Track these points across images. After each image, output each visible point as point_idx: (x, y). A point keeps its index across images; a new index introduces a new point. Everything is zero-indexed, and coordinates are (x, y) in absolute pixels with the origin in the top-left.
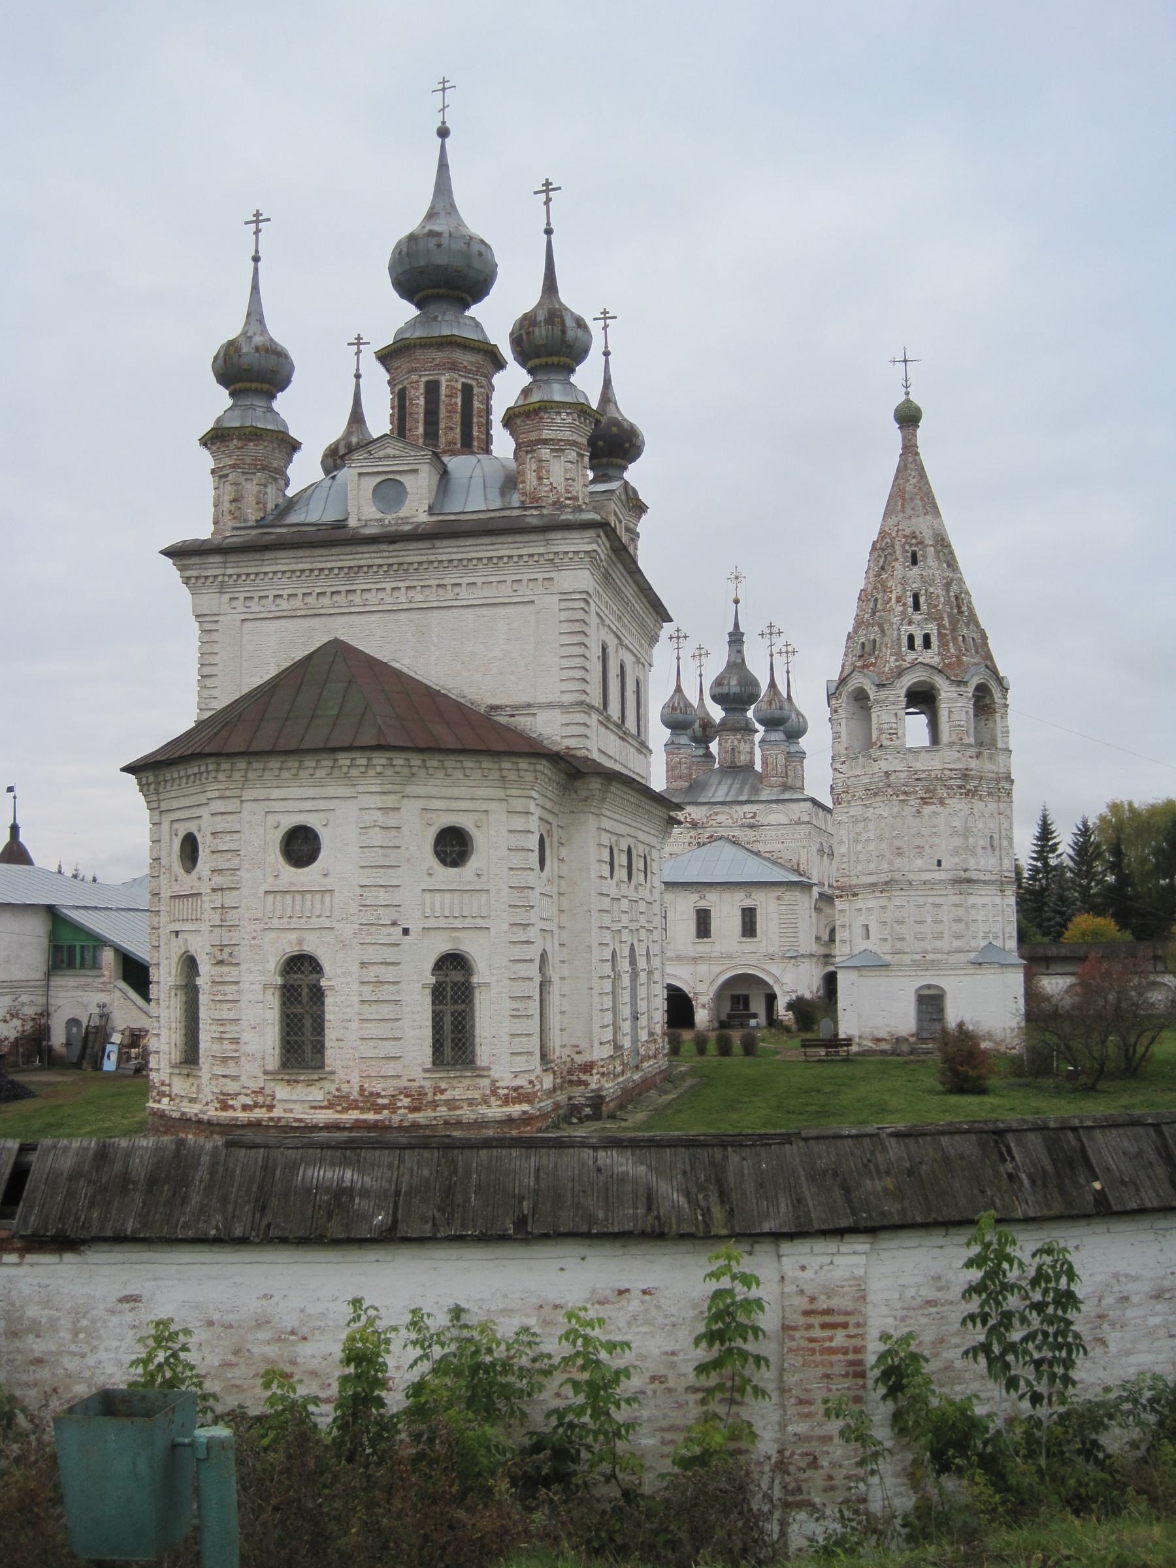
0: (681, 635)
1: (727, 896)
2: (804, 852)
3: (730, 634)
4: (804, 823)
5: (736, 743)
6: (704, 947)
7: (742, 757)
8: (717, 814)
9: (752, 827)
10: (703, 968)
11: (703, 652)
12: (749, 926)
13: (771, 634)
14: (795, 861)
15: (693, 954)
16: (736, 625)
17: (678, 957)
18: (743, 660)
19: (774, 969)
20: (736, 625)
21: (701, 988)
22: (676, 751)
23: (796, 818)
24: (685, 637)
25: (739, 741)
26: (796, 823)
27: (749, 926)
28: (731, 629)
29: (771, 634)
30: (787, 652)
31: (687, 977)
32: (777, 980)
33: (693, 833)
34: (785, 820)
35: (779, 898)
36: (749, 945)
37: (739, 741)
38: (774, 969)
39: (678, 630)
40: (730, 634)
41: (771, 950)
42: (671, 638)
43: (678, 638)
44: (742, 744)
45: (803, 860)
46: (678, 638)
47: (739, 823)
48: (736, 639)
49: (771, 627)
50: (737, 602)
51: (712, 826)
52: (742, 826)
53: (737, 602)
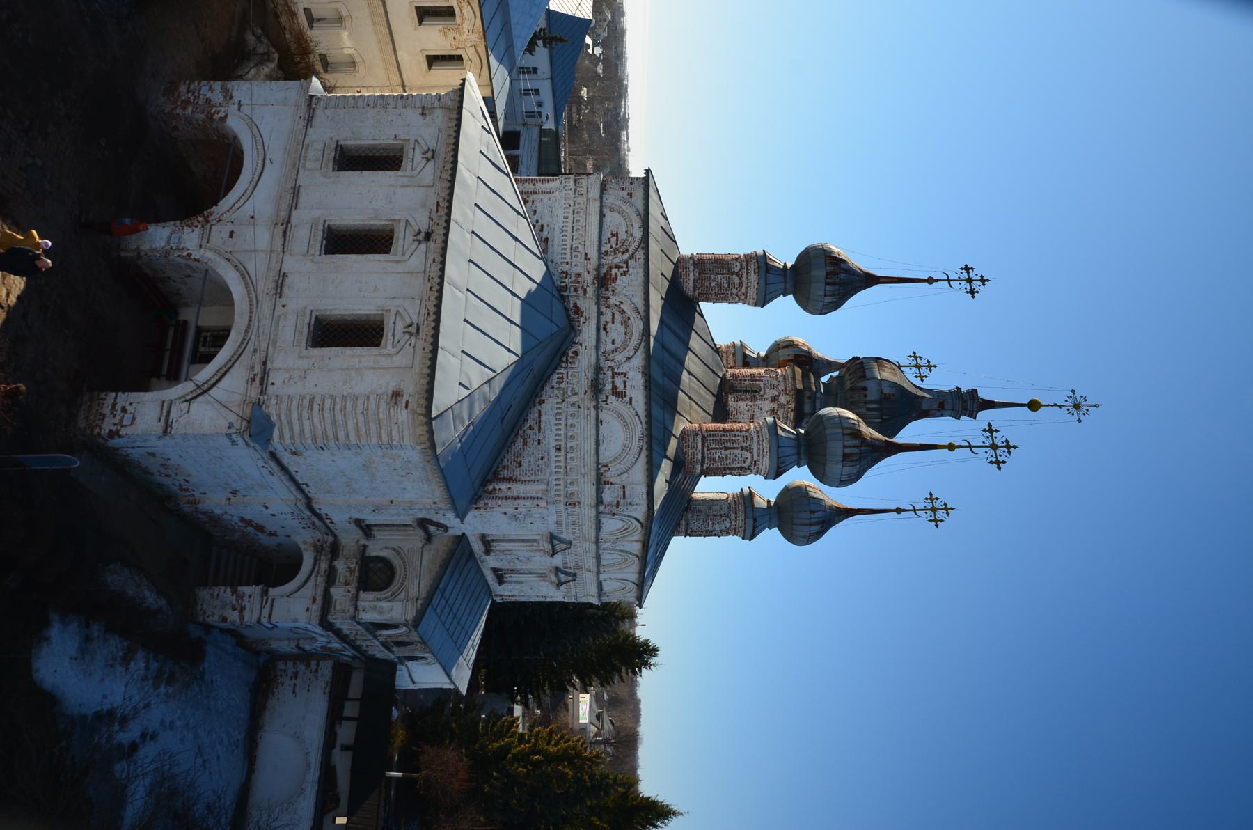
0: (975, 285)
1: (418, 285)
2: (534, 489)
3: (974, 392)
4: (599, 492)
5: (771, 393)
6: (305, 235)
7: (742, 405)
8: (625, 323)
9: (596, 388)
10: (263, 237)
11: (925, 371)
12: (336, 333)
13: (994, 447)
14: (518, 472)
15: (294, 220)
16: (989, 405)
17: (296, 192)
18: (925, 414)
19: (235, 386)
20: (989, 405)
21: (219, 234)
22: (752, 266)
23: (609, 475)
24: (972, 292)
25: (775, 399)
26: (599, 476)
27: (336, 333)
28: (983, 394)
29: (994, 447)
30: (934, 510)
31: (248, 208)
32: (203, 390)
33: (588, 278)
34: (607, 454)
35: (396, 395)
36: (292, 331)
37: (775, 399)
38: (235, 386)
39: (983, 280)
40: (974, 392)
41: (276, 378)
42: (967, 269)
43: (969, 281)
44: (768, 405)
45: (518, 489)
46: (969, 281)
47: (605, 365)
48: (965, 403)
49: (1009, 447)
50: (1034, 405)
51: (600, 314)
52: (598, 369)
53: (1034, 405)
